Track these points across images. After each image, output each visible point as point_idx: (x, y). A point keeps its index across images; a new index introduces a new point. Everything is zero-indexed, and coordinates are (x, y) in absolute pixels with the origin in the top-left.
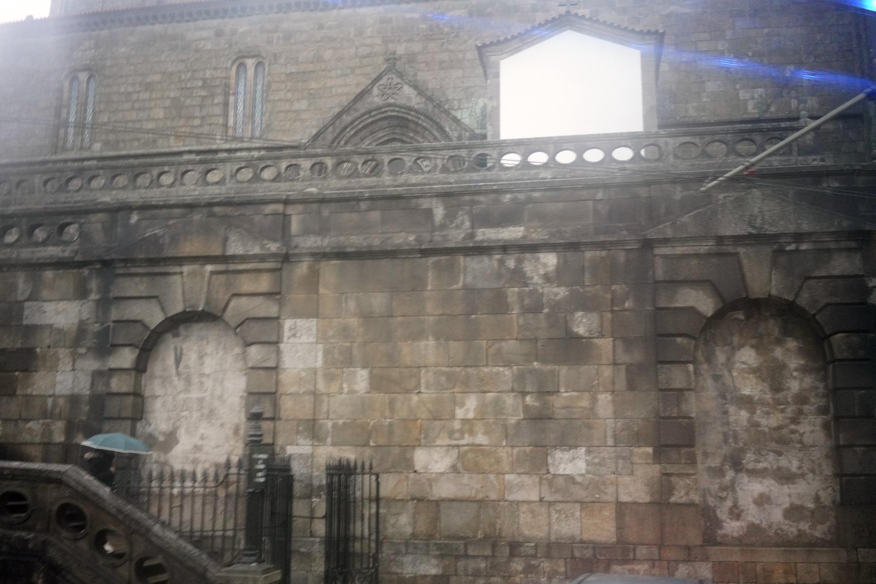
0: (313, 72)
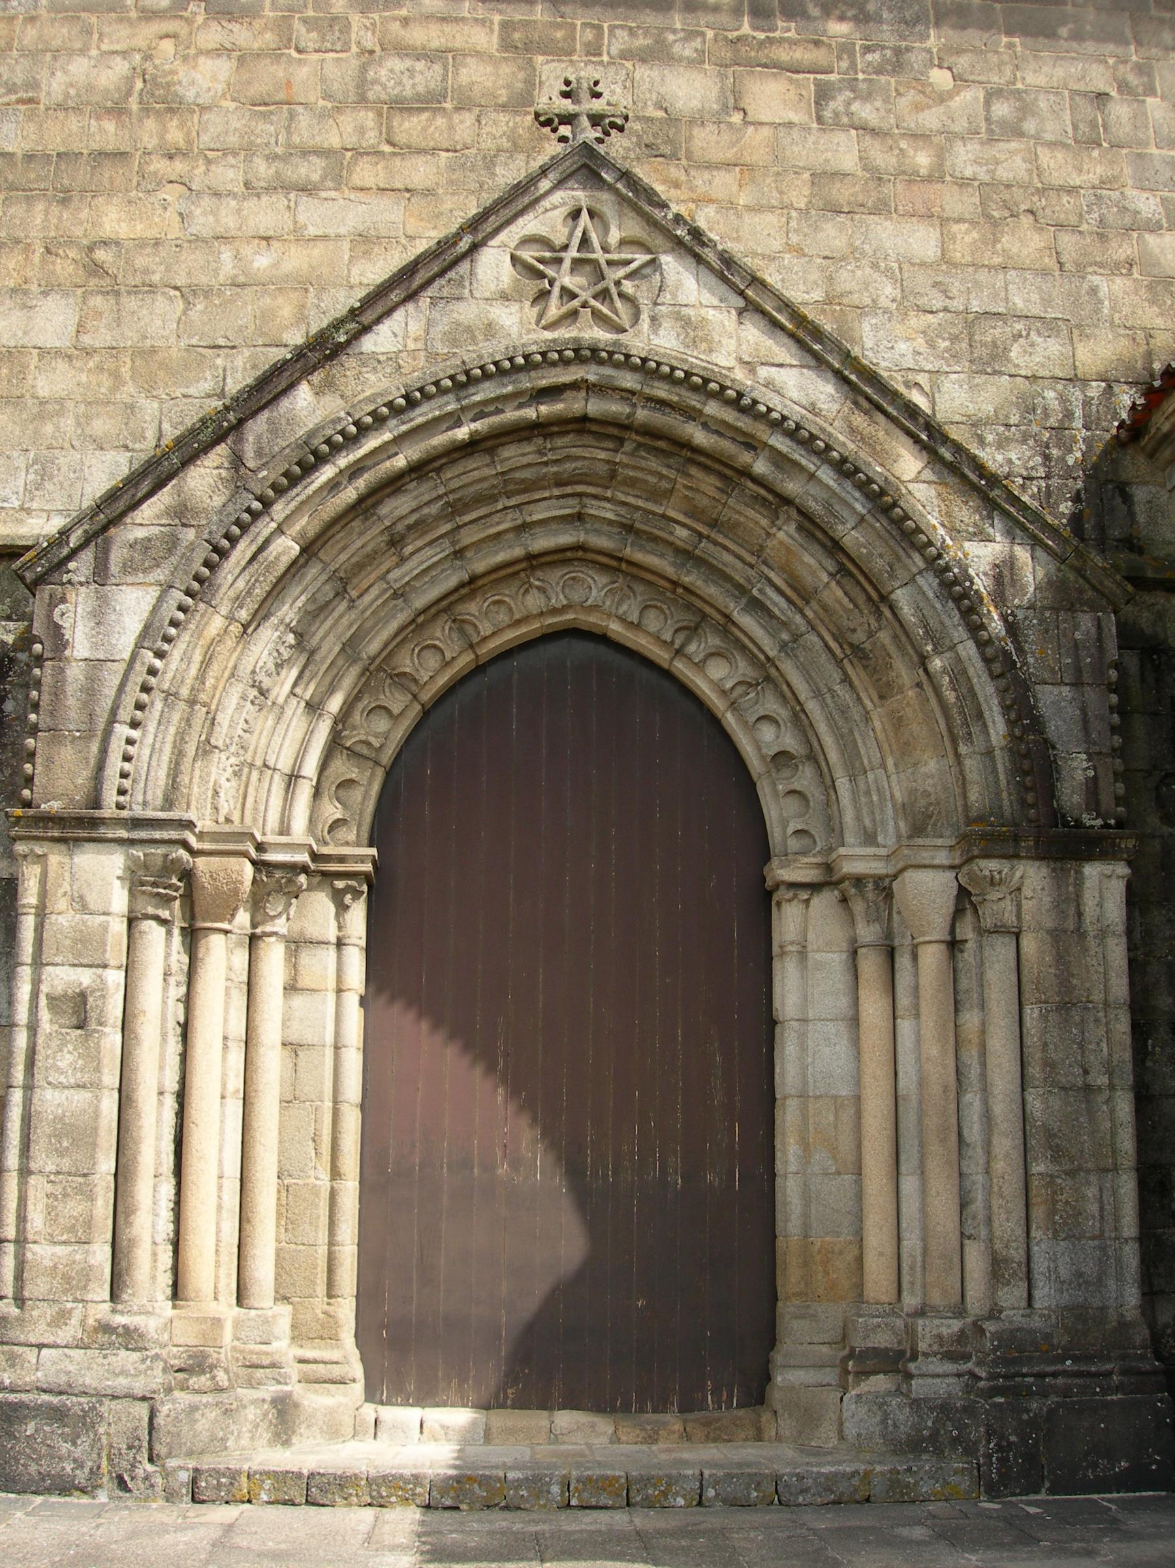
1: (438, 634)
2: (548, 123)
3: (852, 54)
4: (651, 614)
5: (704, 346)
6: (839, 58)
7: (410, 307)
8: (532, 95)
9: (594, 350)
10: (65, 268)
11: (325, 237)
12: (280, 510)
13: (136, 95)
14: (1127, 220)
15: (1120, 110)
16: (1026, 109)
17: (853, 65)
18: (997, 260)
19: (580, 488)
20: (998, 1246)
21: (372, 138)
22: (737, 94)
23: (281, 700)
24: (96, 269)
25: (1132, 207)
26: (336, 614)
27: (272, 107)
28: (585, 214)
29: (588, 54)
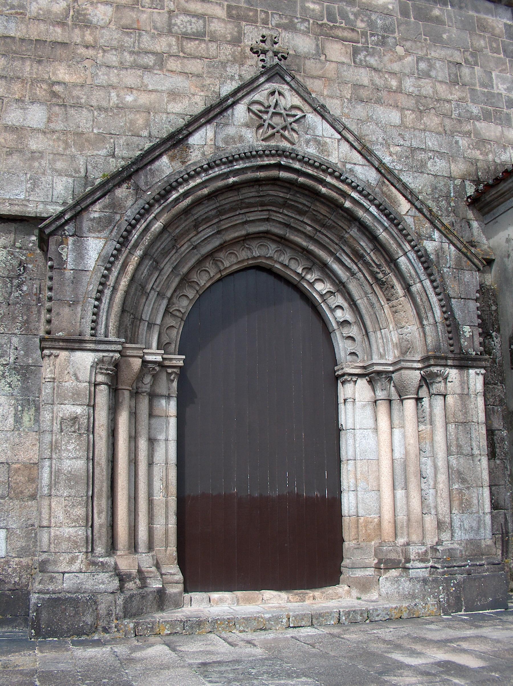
0: (64, 44)
1: (207, 265)
2: (256, 52)
3: (366, 36)
4: (293, 262)
5: (326, 153)
6: (362, 38)
7: (208, 126)
8: (241, 39)
9: (284, 152)
10: (41, 91)
11: (156, 91)
12: (157, 209)
13: (70, 17)
14: (469, 115)
15: (466, 71)
16: (431, 66)
17: (367, 41)
18: (422, 127)
19: (269, 208)
20: (440, 517)
21: (174, 49)
22: (323, 48)
23: (148, 291)
24: (55, 94)
25: (470, 110)
26: (171, 255)
27: (132, 31)
28: (277, 93)
29: (263, 23)
